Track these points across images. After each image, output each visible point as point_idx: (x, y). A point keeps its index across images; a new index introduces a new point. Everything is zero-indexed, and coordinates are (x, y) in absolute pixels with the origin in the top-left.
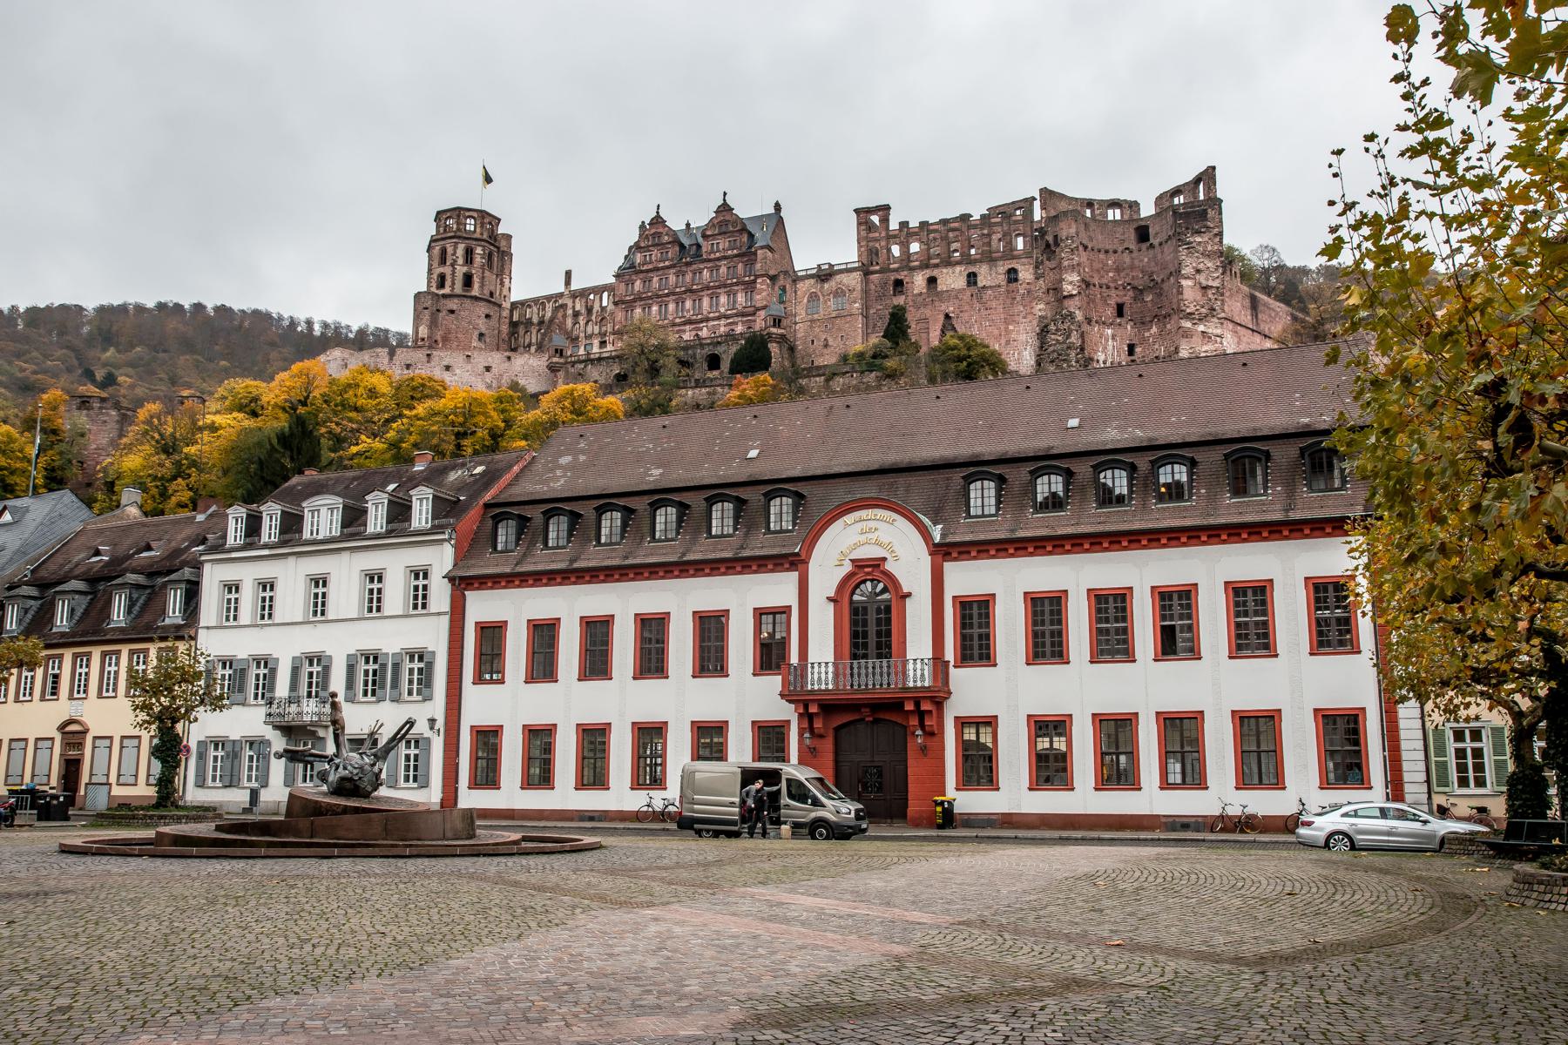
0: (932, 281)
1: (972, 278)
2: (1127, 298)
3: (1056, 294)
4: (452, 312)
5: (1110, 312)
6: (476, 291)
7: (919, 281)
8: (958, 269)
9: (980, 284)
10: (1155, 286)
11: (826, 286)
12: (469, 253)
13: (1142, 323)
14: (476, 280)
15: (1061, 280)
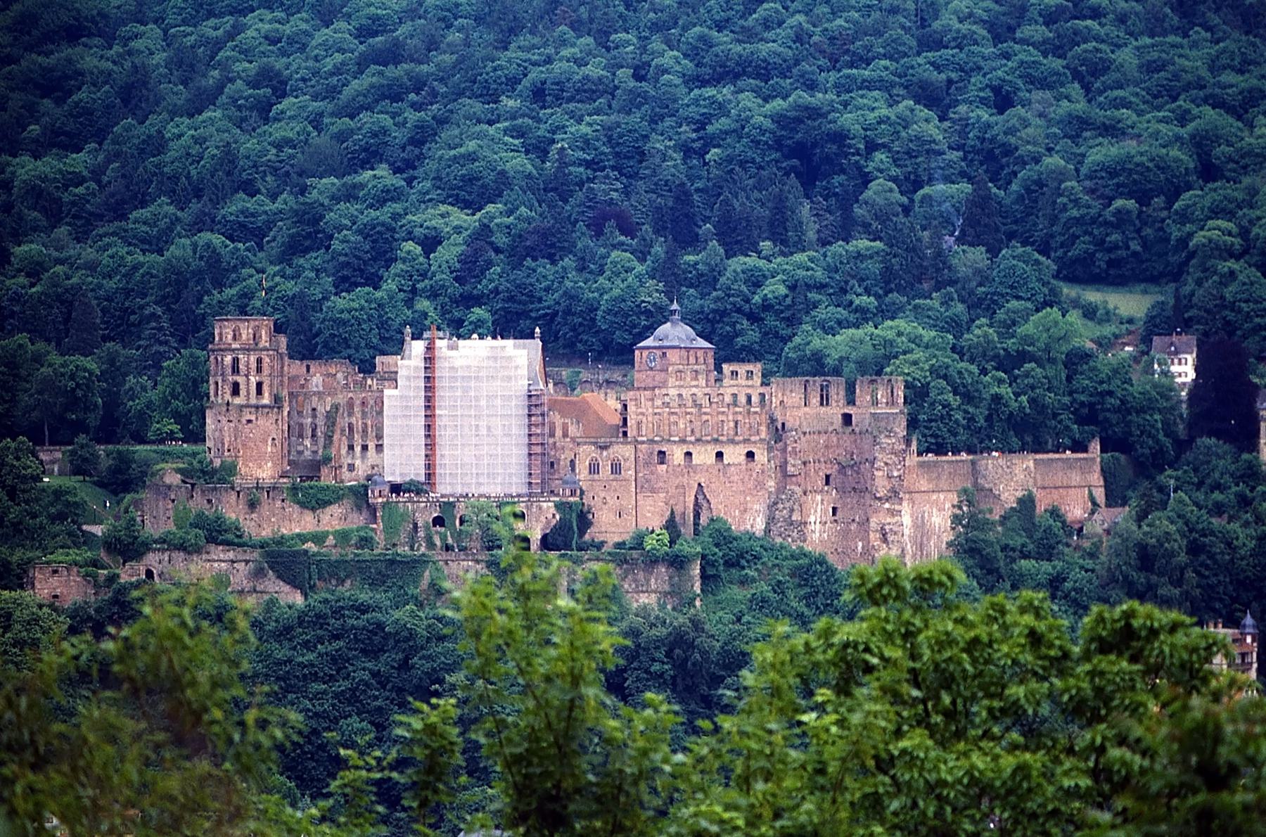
0: (689, 454)
1: (719, 455)
2: (833, 470)
3: (783, 467)
4: (249, 421)
5: (820, 483)
6: (266, 400)
7: (677, 454)
8: (709, 447)
9: (726, 462)
10: (855, 466)
11: (605, 453)
12: (259, 361)
13: (841, 491)
14: (266, 388)
15: (786, 462)
